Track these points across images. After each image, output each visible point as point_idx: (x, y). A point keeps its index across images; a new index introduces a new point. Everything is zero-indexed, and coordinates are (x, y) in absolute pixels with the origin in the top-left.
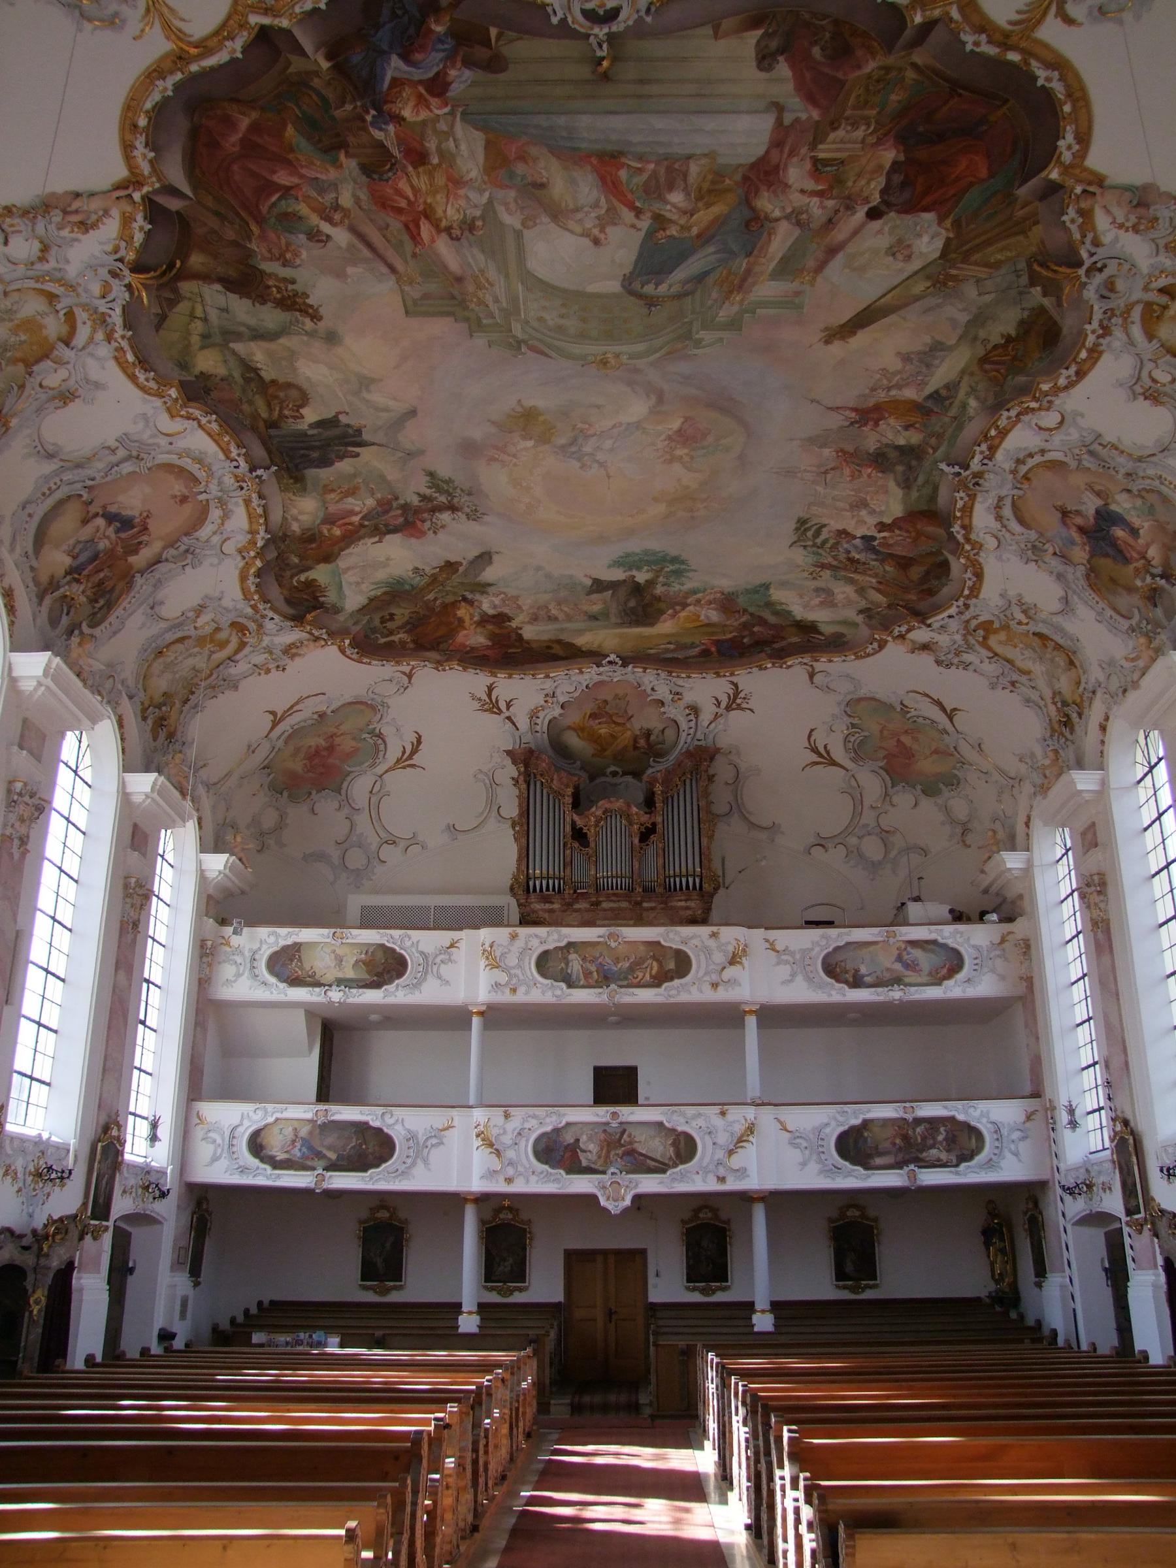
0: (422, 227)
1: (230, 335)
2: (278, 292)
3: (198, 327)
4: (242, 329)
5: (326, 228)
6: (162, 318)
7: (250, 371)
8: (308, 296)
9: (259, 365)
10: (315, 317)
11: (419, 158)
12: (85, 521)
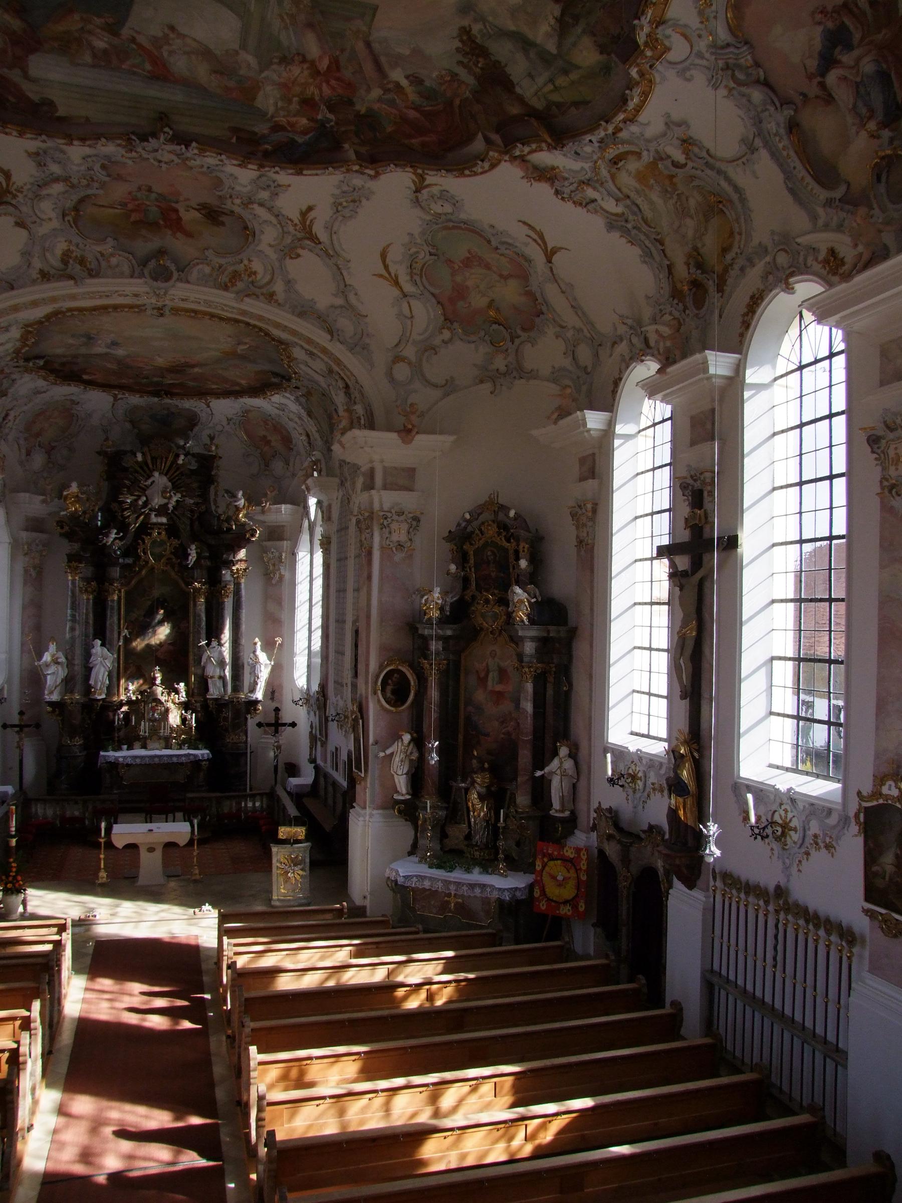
0: (325, 67)
1: (546, 59)
2: (478, 62)
3: (561, 81)
4: (532, 55)
5: (404, 83)
6: (576, 104)
7: (563, 27)
8: (458, 50)
9: (553, 22)
10: (465, 32)
11: (308, 103)
12: (828, 99)
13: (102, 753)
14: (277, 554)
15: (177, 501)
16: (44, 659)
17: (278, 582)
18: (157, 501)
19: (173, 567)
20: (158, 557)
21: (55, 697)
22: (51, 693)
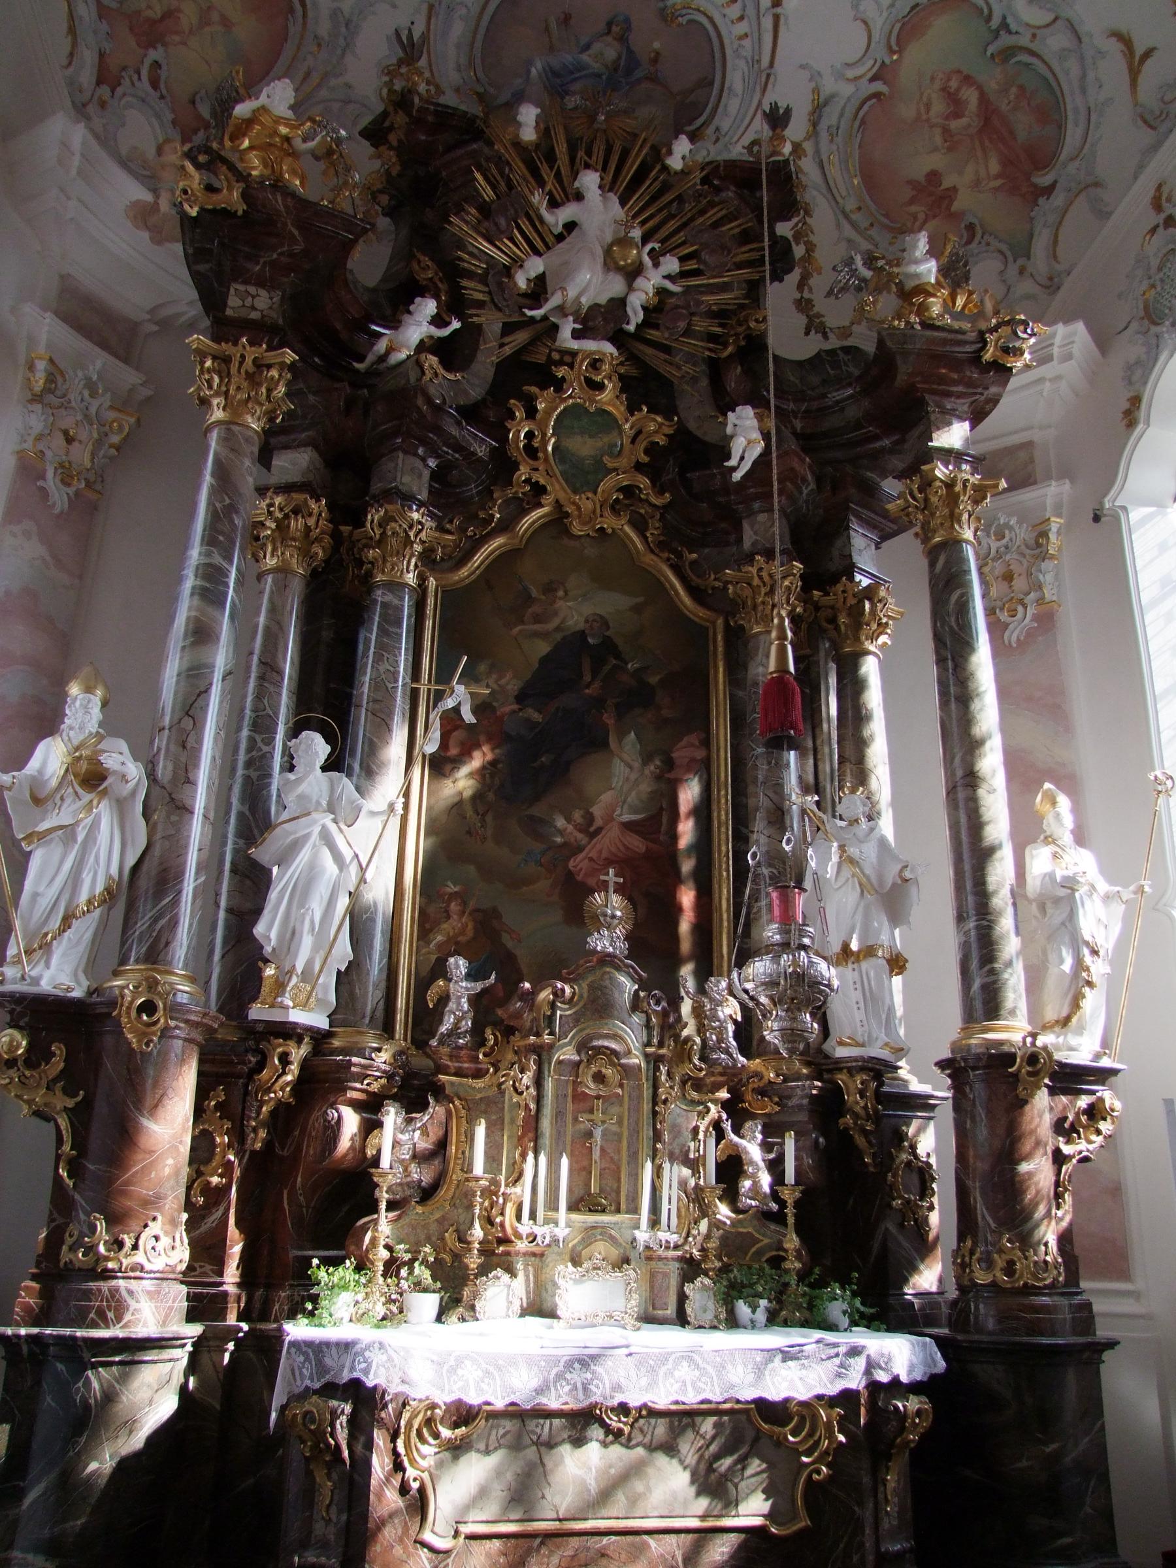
13: (297, 1330)
14: (1022, 534)
15: (661, 292)
16: (34, 764)
17: (1030, 634)
18: (587, 283)
19: (640, 526)
20: (583, 476)
21: (59, 974)
22: (41, 947)
